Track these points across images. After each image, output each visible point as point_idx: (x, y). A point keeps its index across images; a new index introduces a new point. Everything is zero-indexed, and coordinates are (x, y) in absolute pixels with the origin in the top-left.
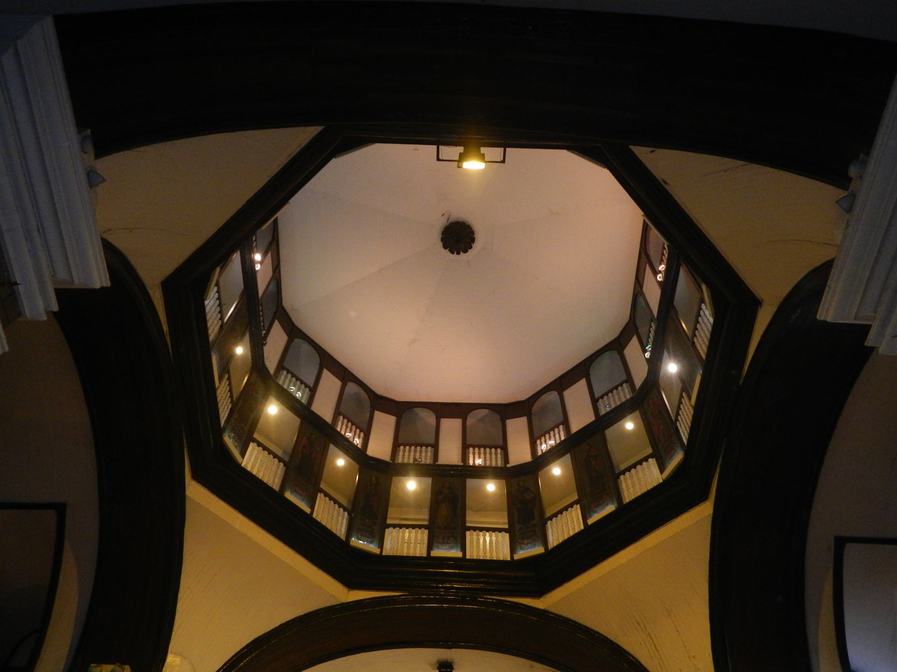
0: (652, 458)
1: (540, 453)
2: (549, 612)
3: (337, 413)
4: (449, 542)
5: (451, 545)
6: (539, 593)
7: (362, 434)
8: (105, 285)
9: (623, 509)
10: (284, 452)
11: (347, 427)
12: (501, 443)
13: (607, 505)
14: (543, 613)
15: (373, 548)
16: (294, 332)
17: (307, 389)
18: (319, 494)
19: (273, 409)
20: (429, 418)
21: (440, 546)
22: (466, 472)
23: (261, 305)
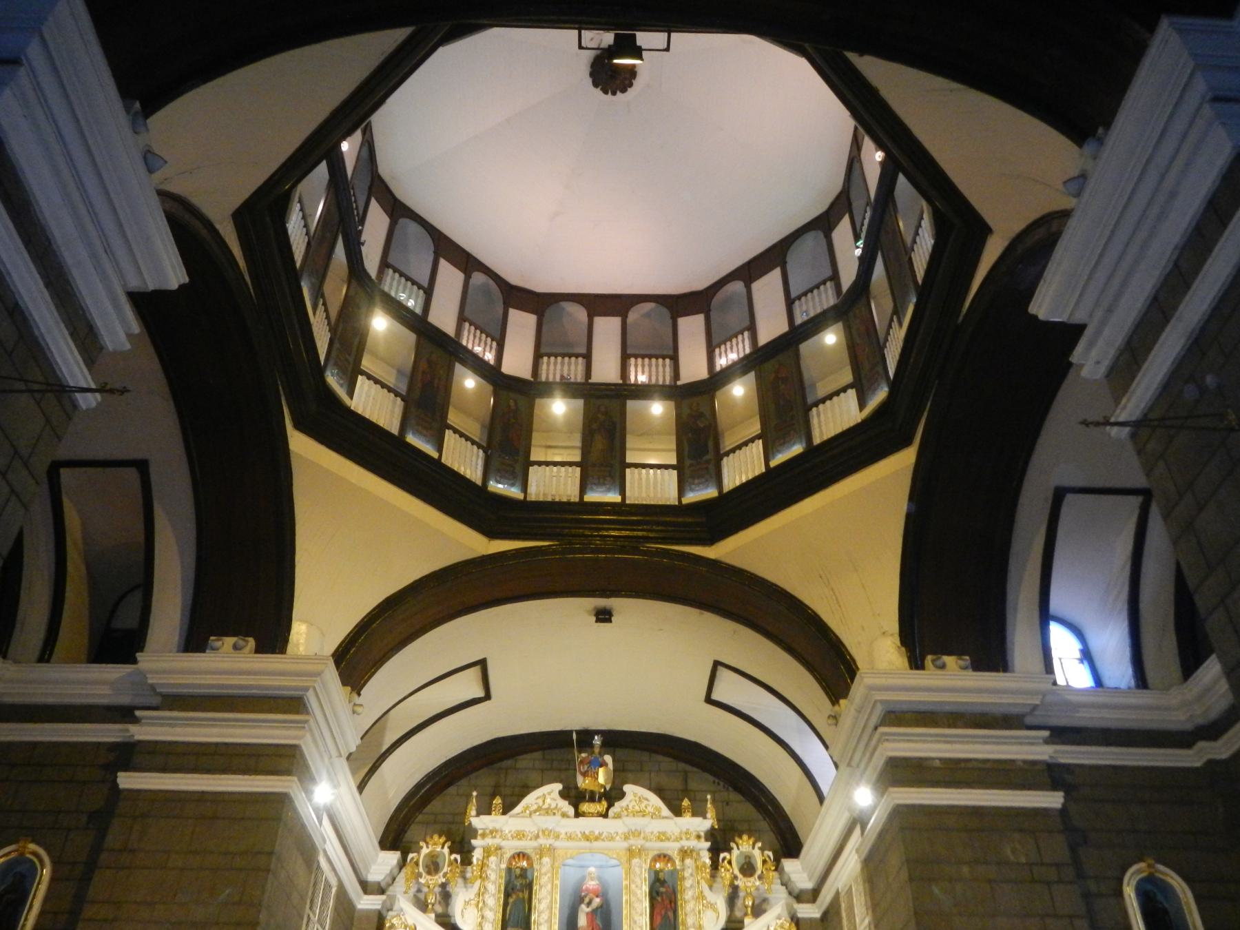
0: (852, 388)
1: (718, 368)
2: (721, 562)
3: (462, 319)
4: (606, 482)
5: (608, 486)
6: (711, 541)
7: (494, 344)
8: (182, 282)
9: (812, 452)
10: (400, 372)
11: (475, 336)
12: (671, 353)
13: (794, 444)
14: (715, 564)
15: (514, 492)
16: (398, 210)
17: (421, 292)
18: (447, 431)
19: (380, 323)
20: (580, 313)
21: (595, 487)
22: (625, 392)
23: (353, 188)
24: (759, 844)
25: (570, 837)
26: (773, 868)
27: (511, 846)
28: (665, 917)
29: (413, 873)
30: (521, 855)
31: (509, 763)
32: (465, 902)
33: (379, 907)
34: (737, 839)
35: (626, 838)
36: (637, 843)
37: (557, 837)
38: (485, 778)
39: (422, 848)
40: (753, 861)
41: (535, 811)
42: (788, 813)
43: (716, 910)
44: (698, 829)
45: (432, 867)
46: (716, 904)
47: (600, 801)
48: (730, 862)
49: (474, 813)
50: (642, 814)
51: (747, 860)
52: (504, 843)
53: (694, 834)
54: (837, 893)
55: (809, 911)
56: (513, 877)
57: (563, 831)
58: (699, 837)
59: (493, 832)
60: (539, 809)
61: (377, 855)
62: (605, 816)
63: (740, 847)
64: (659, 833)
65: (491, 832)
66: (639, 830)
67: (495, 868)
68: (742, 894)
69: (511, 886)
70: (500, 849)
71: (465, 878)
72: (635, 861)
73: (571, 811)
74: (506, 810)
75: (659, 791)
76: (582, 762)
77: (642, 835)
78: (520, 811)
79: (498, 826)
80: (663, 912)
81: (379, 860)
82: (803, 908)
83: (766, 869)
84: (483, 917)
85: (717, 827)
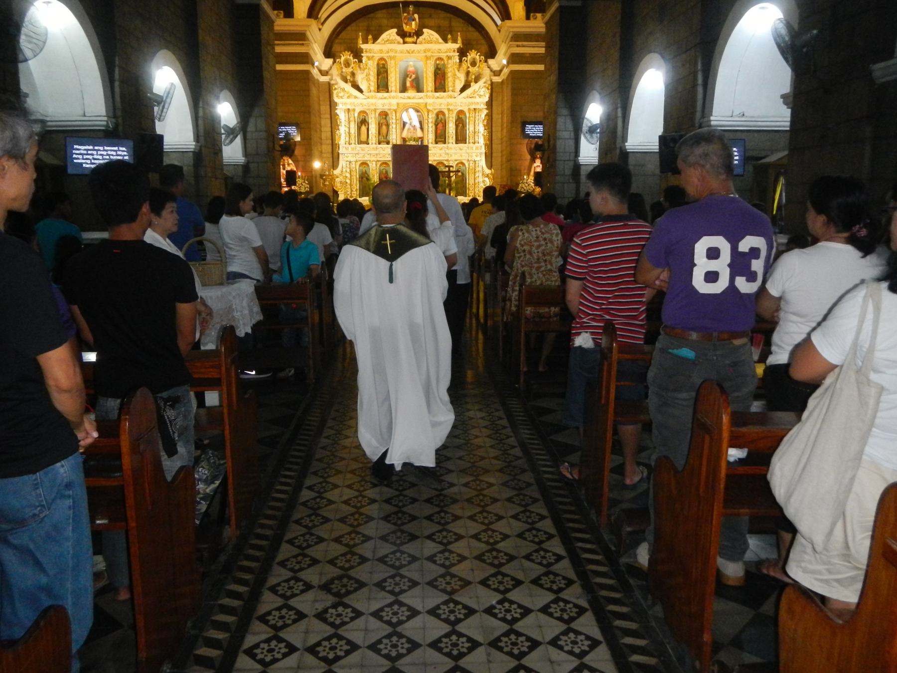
24: (479, 54)
25: (401, 52)
27: (377, 56)
30: (382, 59)
31: (372, 15)
35: (425, 52)
36: (429, 54)
37: (396, 52)
38: (363, 23)
41: (387, 41)
43: (460, 80)
47: (413, 37)
48: (467, 61)
49: (361, 42)
50: (430, 42)
52: (374, 55)
55: (497, 79)
58: (454, 51)
59: (370, 51)
60: (388, 40)
62: (415, 43)
71: (359, 67)
73: (401, 41)
74: (375, 39)
75: (438, 32)
79: (371, 48)
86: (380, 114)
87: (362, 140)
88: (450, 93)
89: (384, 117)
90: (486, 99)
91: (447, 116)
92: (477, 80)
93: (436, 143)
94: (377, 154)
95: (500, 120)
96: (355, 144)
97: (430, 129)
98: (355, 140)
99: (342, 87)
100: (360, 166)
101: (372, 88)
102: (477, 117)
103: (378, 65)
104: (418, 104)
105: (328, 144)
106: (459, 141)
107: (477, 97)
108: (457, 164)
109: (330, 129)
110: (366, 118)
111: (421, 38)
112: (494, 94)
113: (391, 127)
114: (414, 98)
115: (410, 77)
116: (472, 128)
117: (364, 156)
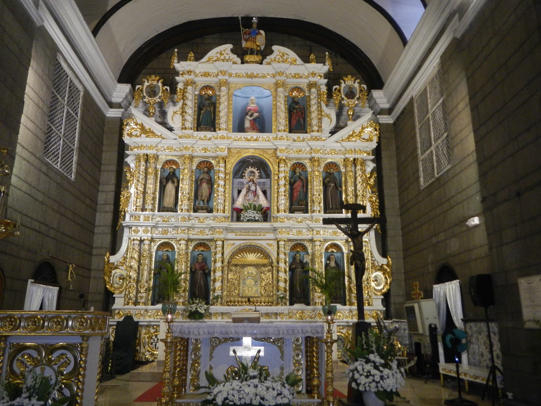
24: (358, 81)
26: (366, 94)
27: (201, 81)
28: (299, 121)
29: (139, 96)
31: (199, 40)
32: (174, 112)
33: (120, 116)
34: (344, 78)
35: (274, 76)
37: (230, 76)
39: (145, 82)
40: (354, 90)
41: (215, 61)
42: (375, 65)
44: (320, 72)
45: (152, 93)
46: (330, 114)
47: (257, 54)
48: (339, 91)
49: (176, 61)
51: (351, 89)
52: (196, 79)
53: (317, 74)
54: (412, 99)
56: (204, 100)
57: (234, 72)
58: (321, 76)
59: (189, 72)
61: (116, 86)
62: (261, 63)
63: (346, 82)
64: (295, 74)
65: (188, 72)
66: (282, 72)
67: (191, 93)
68: (344, 113)
69: (202, 105)
70: (194, 83)
72: (280, 89)
73: (239, 60)
76: (245, 33)
77: (284, 75)
78: (206, 60)
80: (297, 119)
81: (117, 89)
82: (382, 118)
83: (362, 95)
84: (185, 120)
85: (331, 70)
86: (198, 167)
87: (166, 204)
88: (315, 134)
89: (206, 169)
90: (374, 145)
91: (309, 170)
92: (356, 117)
93: (292, 211)
94: (189, 228)
95: (396, 179)
96: (152, 210)
97: (282, 189)
98: (153, 204)
99: (139, 122)
100: (158, 250)
101: (188, 125)
102: (359, 173)
103: (200, 96)
104: (264, 150)
105: (107, 212)
106: (329, 210)
107: (358, 141)
108: (327, 249)
109: (112, 188)
110: (177, 173)
111: (268, 59)
112: (383, 141)
113: (215, 186)
114: (256, 140)
115: (251, 116)
116: (351, 189)
117: (165, 232)
